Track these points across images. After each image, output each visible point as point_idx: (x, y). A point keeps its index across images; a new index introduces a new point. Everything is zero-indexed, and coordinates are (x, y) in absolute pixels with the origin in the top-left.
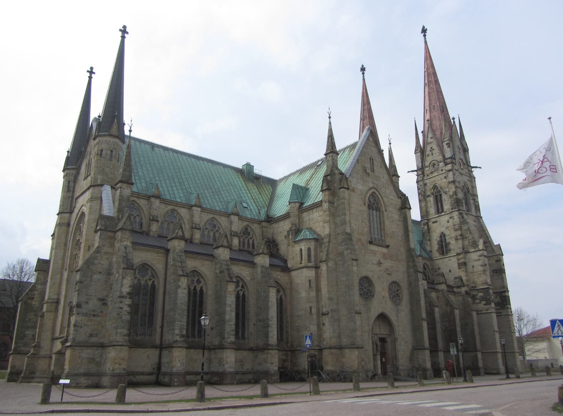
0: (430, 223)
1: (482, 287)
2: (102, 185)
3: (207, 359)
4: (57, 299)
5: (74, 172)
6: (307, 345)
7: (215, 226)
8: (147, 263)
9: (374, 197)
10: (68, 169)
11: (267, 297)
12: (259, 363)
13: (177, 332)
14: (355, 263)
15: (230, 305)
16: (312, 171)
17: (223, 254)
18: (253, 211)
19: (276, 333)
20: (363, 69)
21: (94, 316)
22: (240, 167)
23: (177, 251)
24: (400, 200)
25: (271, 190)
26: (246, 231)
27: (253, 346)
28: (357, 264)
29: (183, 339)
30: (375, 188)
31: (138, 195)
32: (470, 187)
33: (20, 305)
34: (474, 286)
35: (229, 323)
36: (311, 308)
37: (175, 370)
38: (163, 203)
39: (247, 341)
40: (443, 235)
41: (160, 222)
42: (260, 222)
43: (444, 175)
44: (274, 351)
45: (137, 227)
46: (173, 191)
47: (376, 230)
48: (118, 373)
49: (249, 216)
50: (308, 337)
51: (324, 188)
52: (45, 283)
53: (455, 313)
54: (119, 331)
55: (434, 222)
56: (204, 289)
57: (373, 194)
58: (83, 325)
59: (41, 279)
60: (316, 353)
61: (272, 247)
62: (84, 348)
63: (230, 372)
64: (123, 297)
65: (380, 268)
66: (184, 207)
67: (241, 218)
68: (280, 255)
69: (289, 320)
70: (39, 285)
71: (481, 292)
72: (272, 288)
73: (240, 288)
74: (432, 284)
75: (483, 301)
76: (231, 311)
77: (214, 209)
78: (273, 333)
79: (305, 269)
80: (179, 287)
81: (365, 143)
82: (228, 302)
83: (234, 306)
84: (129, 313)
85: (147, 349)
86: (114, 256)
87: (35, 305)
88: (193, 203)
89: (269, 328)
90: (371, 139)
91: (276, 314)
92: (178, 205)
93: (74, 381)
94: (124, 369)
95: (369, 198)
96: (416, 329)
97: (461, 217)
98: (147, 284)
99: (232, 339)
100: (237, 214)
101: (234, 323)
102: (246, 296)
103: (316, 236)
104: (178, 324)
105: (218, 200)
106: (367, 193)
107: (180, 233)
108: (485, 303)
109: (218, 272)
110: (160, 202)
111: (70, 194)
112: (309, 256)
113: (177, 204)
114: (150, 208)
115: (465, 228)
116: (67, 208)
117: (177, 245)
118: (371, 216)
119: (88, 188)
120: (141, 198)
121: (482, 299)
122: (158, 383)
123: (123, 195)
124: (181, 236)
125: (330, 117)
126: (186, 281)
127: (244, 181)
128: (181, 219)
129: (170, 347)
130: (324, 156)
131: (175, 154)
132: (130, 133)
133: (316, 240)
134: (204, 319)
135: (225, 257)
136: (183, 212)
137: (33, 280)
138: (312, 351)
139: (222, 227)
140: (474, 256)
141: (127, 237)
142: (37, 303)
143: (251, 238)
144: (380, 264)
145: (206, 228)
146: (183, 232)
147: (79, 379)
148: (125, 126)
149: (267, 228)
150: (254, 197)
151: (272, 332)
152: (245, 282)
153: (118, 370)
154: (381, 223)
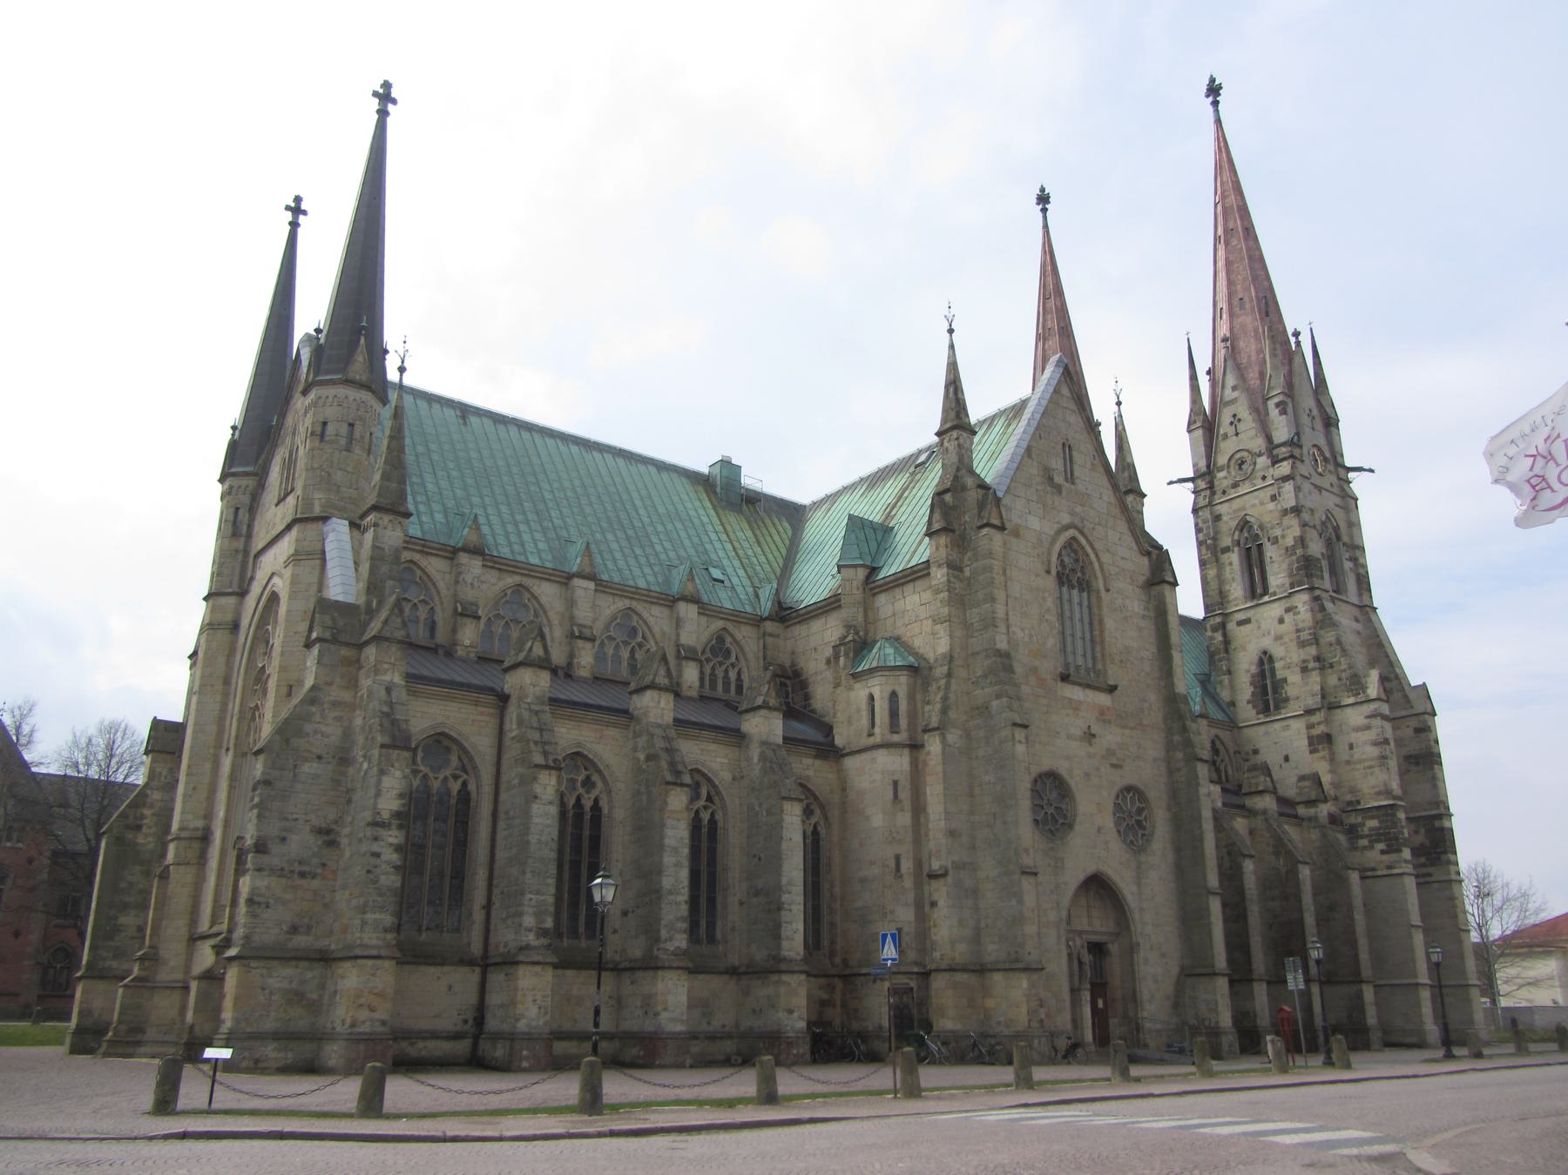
0: (1231, 626)
1: (1376, 804)
2: (325, 519)
3: (610, 997)
4: (204, 829)
5: (250, 483)
6: (887, 960)
7: (633, 632)
8: (447, 731)
9: (1075, 552)
10: (234, 475)
11: (779, 825)
12: (754, 1011)
13: (529, 921)
14: (1020, 734)
15: (675, 850)
16: (903, 479)
17: (656, 708)
18: (739, 589)
19: (801, 927)
20: (1043, 199)
21: (302, 875)
22: (704, 469)
23: (529, 700)
24: (1145, 561)
25: (790, 533)
26: (719, 647)
27: (737, 963)
28: (1027, 738)
29: (544, 941)
30: (1076, 528)
31: (424, 546)
32: (1343, 525)
33: (103, 844)
34: (1353, 799)
35: (671, 898)
36: (898, 859)
37: (522, 1026)
38: (492, 568)
39: (720, 947)
40: (1266, 659)
41: (483, 621)
42: (757, 621)
43: (1270, 492)
45: (420, 634)
46: (519, 534)
47: (1079, 643)
48: (366, 1034)
49: (728, 605)
50: (889, 939)
51: (936, 526)
52: (171, 787)
53: (1300, 876)
54: (370, 916)
55: (1240, 623)
56: (604, 804)
57: (1071, 544)
58: (271, 901)
59: (160, 773)
60: (913, 984)
61: (790, 689)
62: (275, 963)
63: (675, 1033)
64: (383, 825)
65: (1091, 750)
66: (548, 580)
67: (705, 609)
68: (813, 711)
69: (837, 890)
70: (155, 792)
71: (1373, 818)
73: (702, 803)
74: (1235, 795)
75: (1379, 841)
76: (678, 865)
77: (631, 583)
78: (794, 926)
79: (882, 752)
81: (1049, 401)
82: (670, 841)
83: (686, 851)
84: (396, 868)
85: (446, 969)
86: (358, 712)
87: (144, 845)
88: (575, 569)
89: (783, 913)
90: (1065, 391)
91: (802, 874)
92: (532, 574)
93: (246, 1054)
94: (384, 1023)
95: (1060, 555)
96: (1190, 919)
97: (1317, 608)
98: (448, 792)
99: (681, 941)
100: (694, 600)
101: (686, 898)
102: (720, 824)
103: (911, 659)
104: (531, 899)
105: (643, 560)
106: (1054, 540)
107: (538, 651)
108: (1385, 847)
109: (642, 757)
110: (484, 566)
111: (240, 544)
112: (894, 714)
113: (530, 570)
114: (457, 582)
115: (1329, 639)
116: (231, 582)
117: (530, 684)
118: (1066, 606)
119: (289, 528)
120: (432, 554)
121: (1376, 836)
122: (477, 1063)
123: (382, 545)
124: (539, 657)
125: (951, 331)
126: (554, 781)
127: (714, 508)
128: (541, 612)
129: (510, 962)
130: (936, 439)
131: (526, 435)
132: (401, 375)
133: (913, 670)
134: (601, 884)
135: (662, 715)
136: (547, 592)
137: (139, 778)
138: (900, 977)
139: (653, 635)
140: (1354, 716)
141: (393, 659)
142: (150, 839)
143: (733, 665)
144: (1089, 736)
145: (610, 638)
146: (545, 648)
147: (263, 1049)
148: (387, 357)
149: (778, 636)
150: (741, 552)
151: (791, 923)
152: (715, 786)
153: (368, 1023)
154: (1094, 623)
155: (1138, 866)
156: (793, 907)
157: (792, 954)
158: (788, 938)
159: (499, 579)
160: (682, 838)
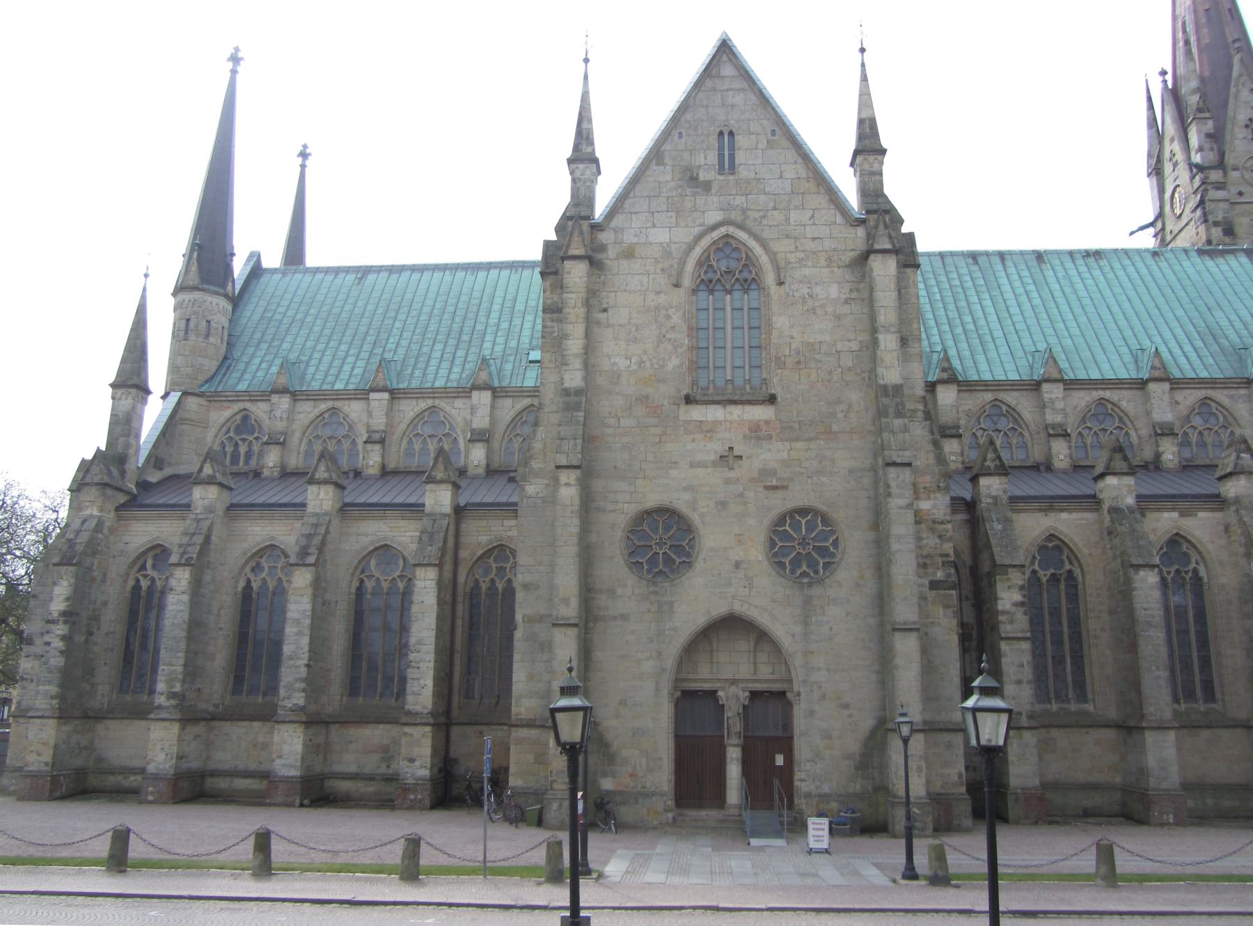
15: (297, 621)
19: (430, 683)
29: (173, 702)
35: (291, 662)
44: (419, 728)
54: (41, 688)
63: (287, 777)
65: (731, 474)
72: (423, 569)
76: (299, 633)
78: (422, 682)
80: (171, 590)
84: (62, 652)
91: (433, 634)
94: (47, 764)
99: (299, 699)
151: (418, 679)
155: (808, 601)
156: (421, 665)
157: (418, 708)
158: (414, 693)
159: (315, 407)
160: (304, 611)
